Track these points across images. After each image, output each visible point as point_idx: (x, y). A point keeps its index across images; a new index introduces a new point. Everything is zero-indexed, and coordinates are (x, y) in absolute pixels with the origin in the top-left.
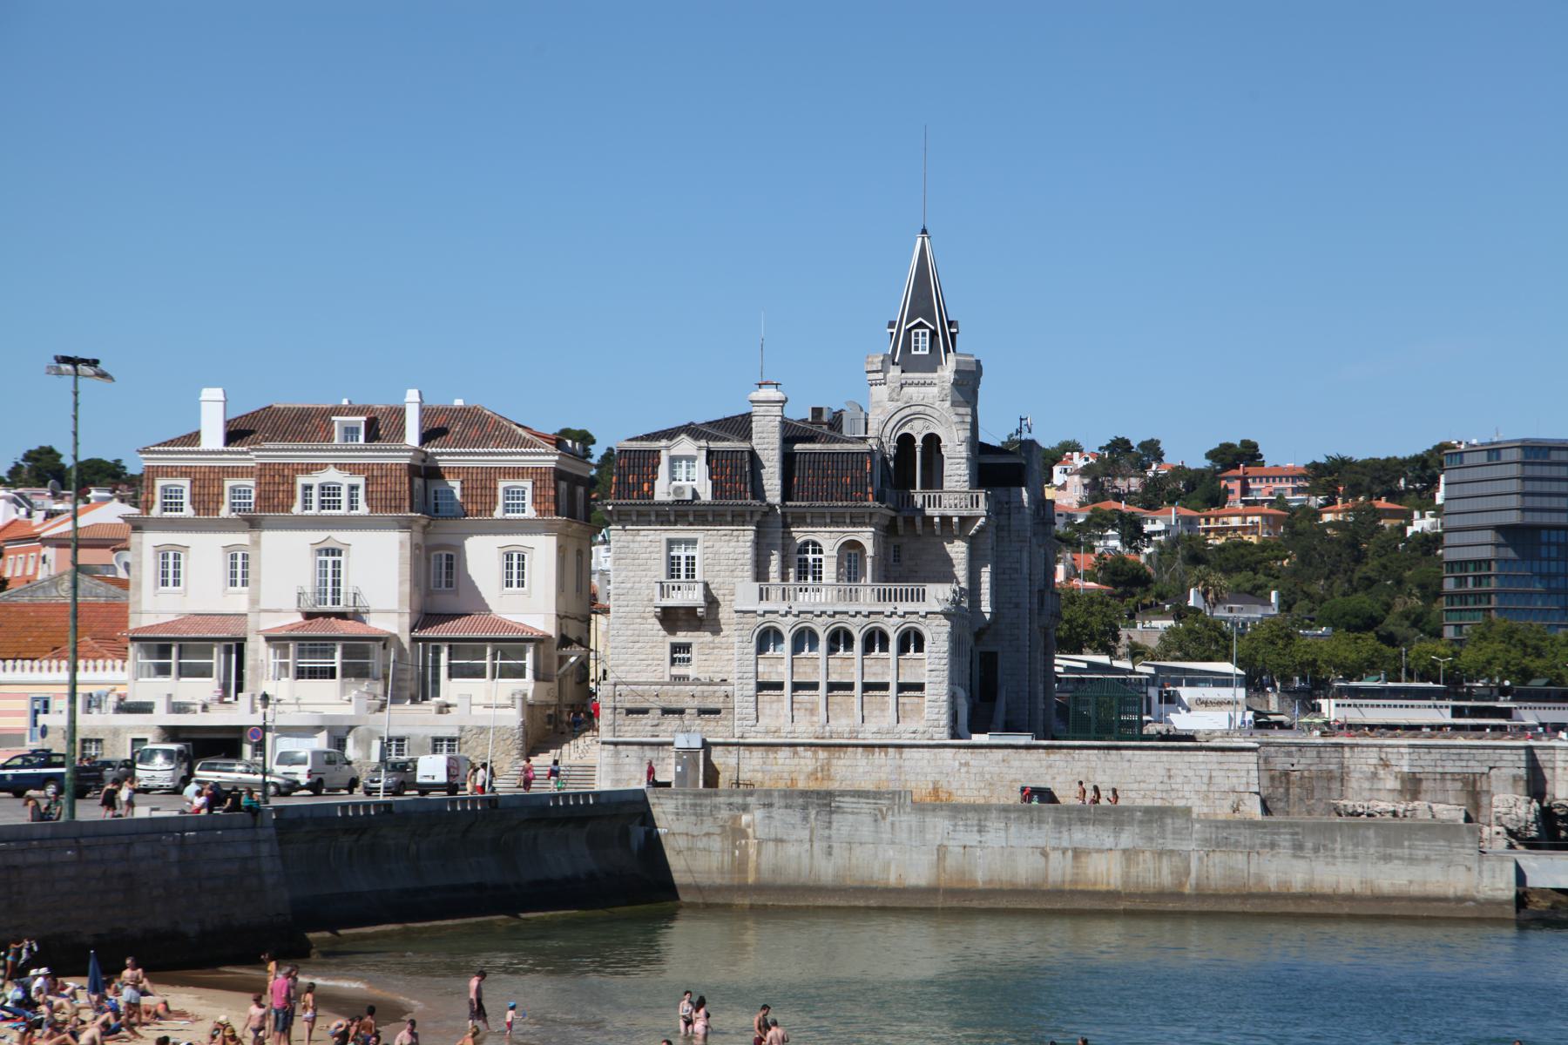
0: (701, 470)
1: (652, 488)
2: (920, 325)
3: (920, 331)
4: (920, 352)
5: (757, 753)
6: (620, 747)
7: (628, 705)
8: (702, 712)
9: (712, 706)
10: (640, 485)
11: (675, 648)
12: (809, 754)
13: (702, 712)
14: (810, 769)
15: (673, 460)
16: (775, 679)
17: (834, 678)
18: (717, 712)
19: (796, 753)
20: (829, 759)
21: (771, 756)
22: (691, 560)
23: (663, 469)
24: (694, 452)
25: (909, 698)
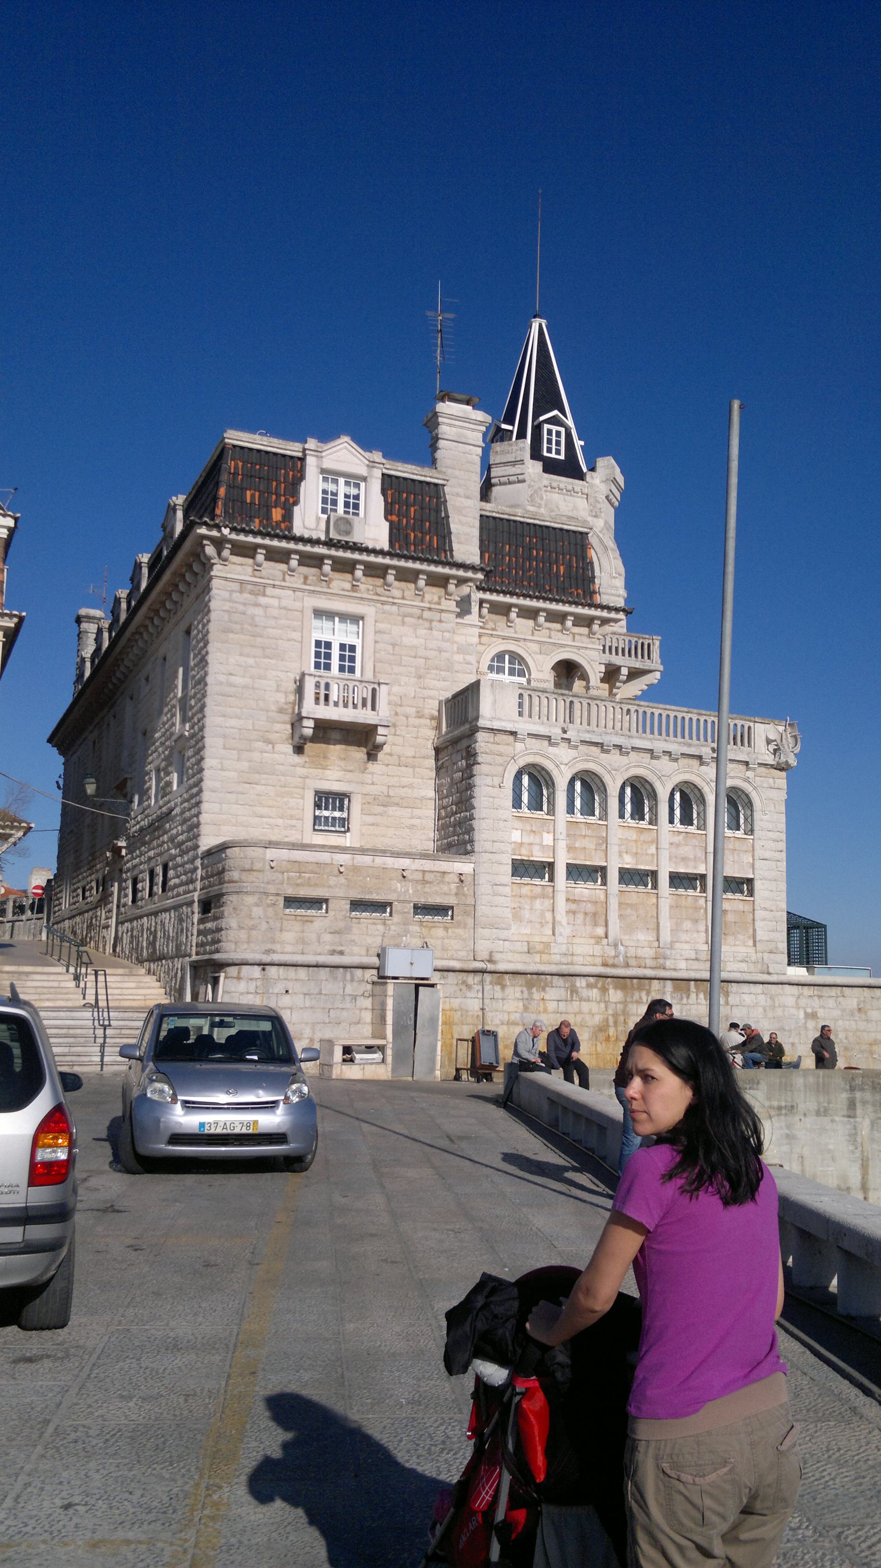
0: (374, 502)
1: (288, 517)
2: (554, 421)
3: (555, 428)
4: (553, 455)
5: (515, 991)
6: (273, 971)
7: (290, 892)
8: (423, 909)
9: (438, 900)
10: (266, 509)
11: (324, 799)
12: (595, 993)
13: (423, 909)
14: (597, 1020)
15: (329, 474)
16: (539, 856)
17: (629, 862)
18: (441, 910)
19: (574, 991)
20: (625, 1003)
21: (537, 995)
22: (348, 650)
23: (311, 489)
24: (362, 471)
25: (732, 902)
